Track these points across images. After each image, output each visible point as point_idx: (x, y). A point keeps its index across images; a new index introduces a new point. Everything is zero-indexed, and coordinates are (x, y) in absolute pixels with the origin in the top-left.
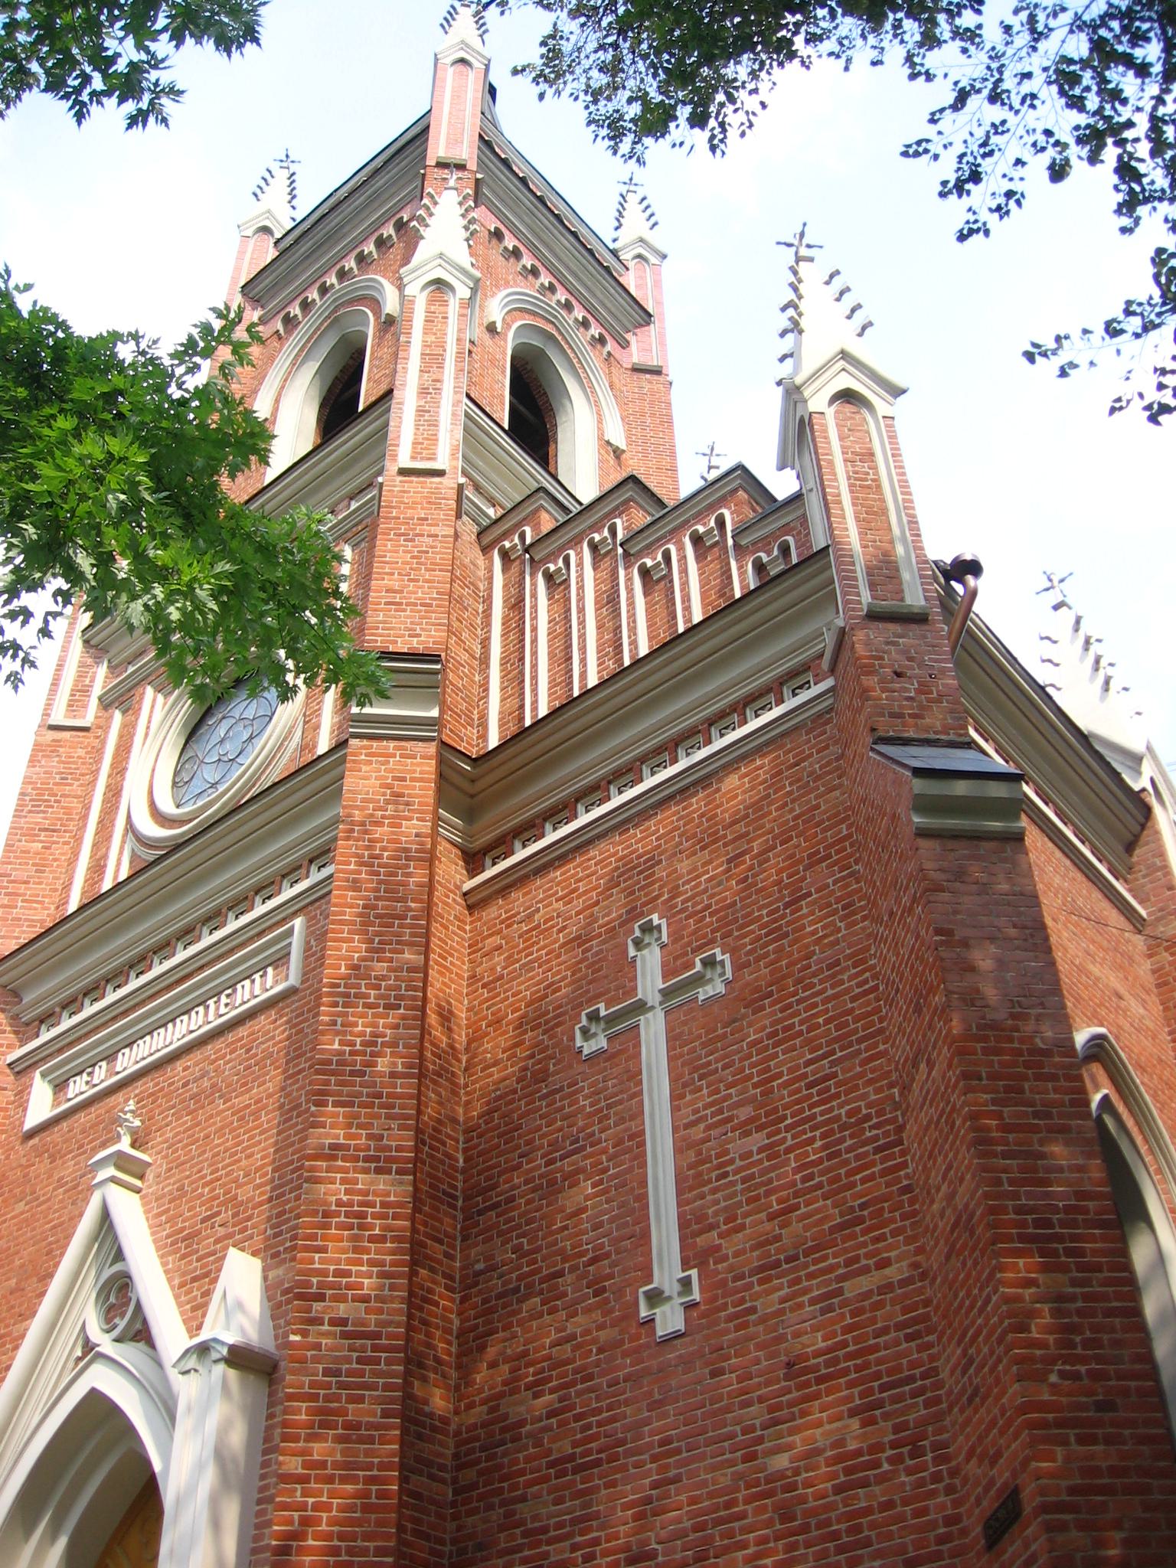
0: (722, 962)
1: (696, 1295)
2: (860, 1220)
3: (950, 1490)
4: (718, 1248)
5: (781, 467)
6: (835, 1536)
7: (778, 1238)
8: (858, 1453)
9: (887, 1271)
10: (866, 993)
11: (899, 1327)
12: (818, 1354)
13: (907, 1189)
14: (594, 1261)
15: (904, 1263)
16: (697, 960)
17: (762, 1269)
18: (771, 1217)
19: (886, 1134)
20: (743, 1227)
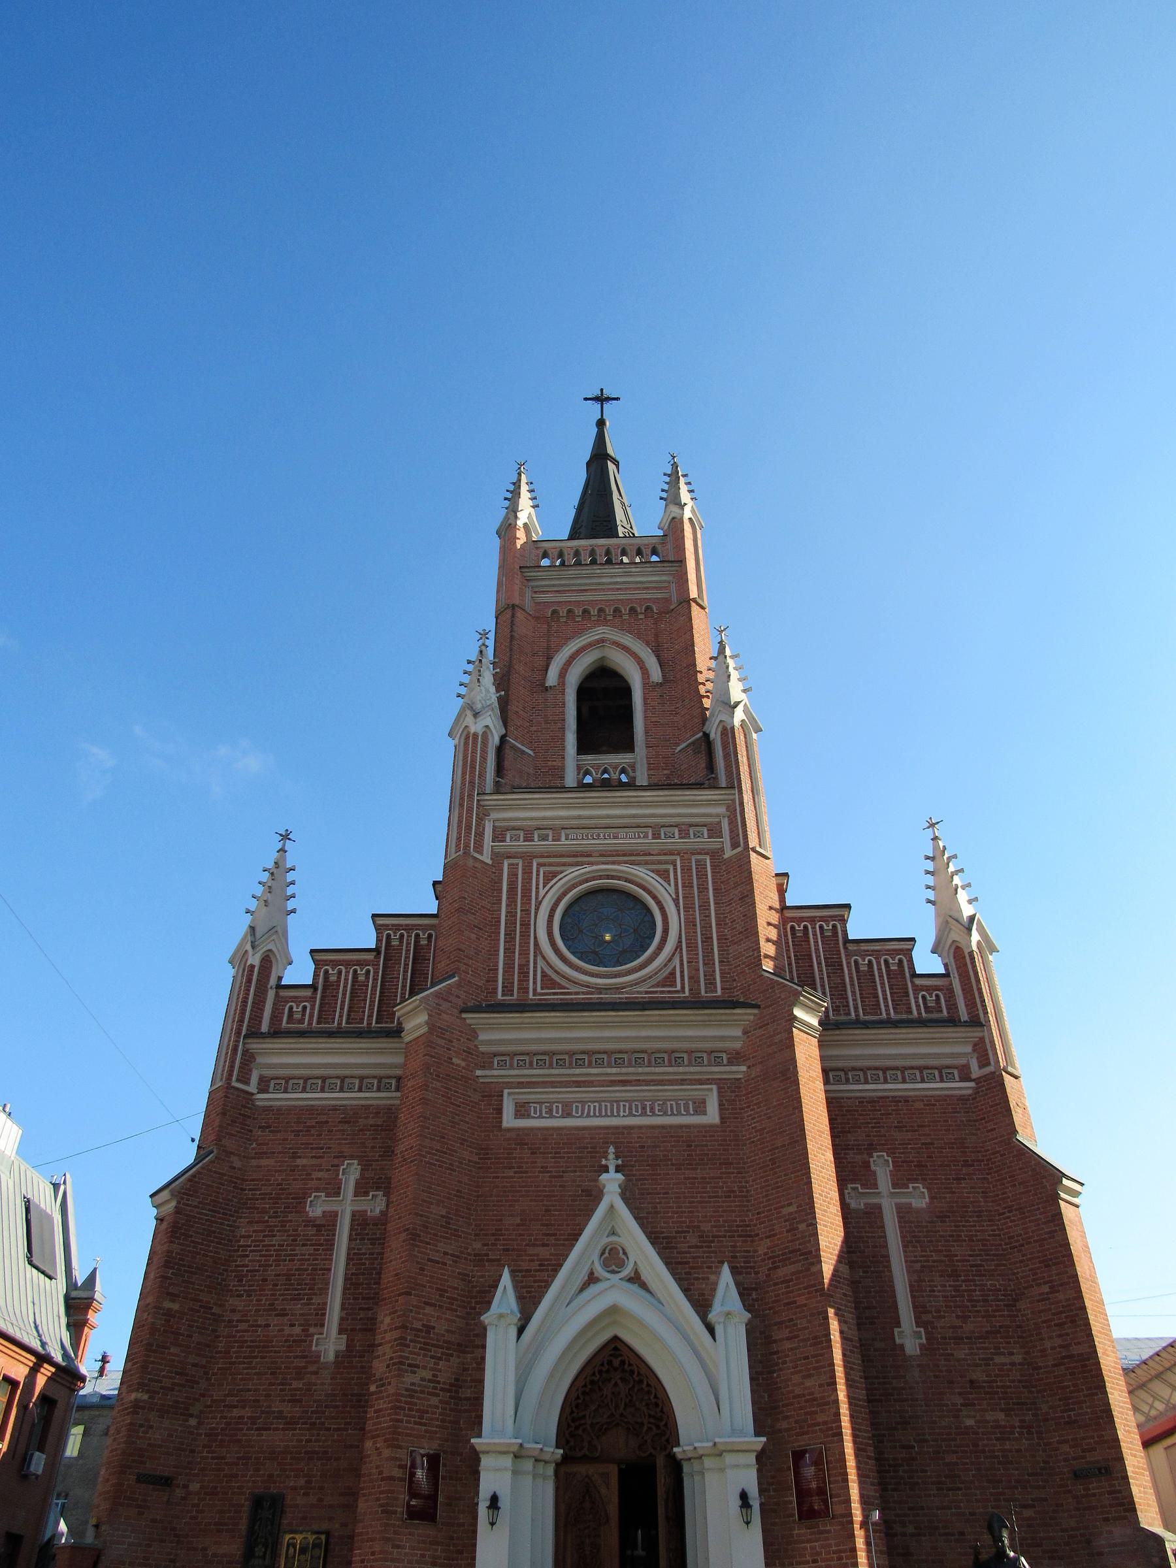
0: (923, 1192)
1: (924, 1341)
2: (1000, 1332)
3: (1044, 1451)
4: (933, 1323)
5: (933, 952)
6: (997, 1457)
7: (962, 1327)
8: (1005, 1427)
9: (1012, 1357)
10: (993, 1235)
11: (1020, 1381)
12: (984, 1382)
13: (1020, 1327)
14: (868, 1308)
15: (1020, 1357)
16: (911, 1185)
17: (955, 1338)
18: (958, 1317)
19: (1008, 1300)
20: (944, 1317)
